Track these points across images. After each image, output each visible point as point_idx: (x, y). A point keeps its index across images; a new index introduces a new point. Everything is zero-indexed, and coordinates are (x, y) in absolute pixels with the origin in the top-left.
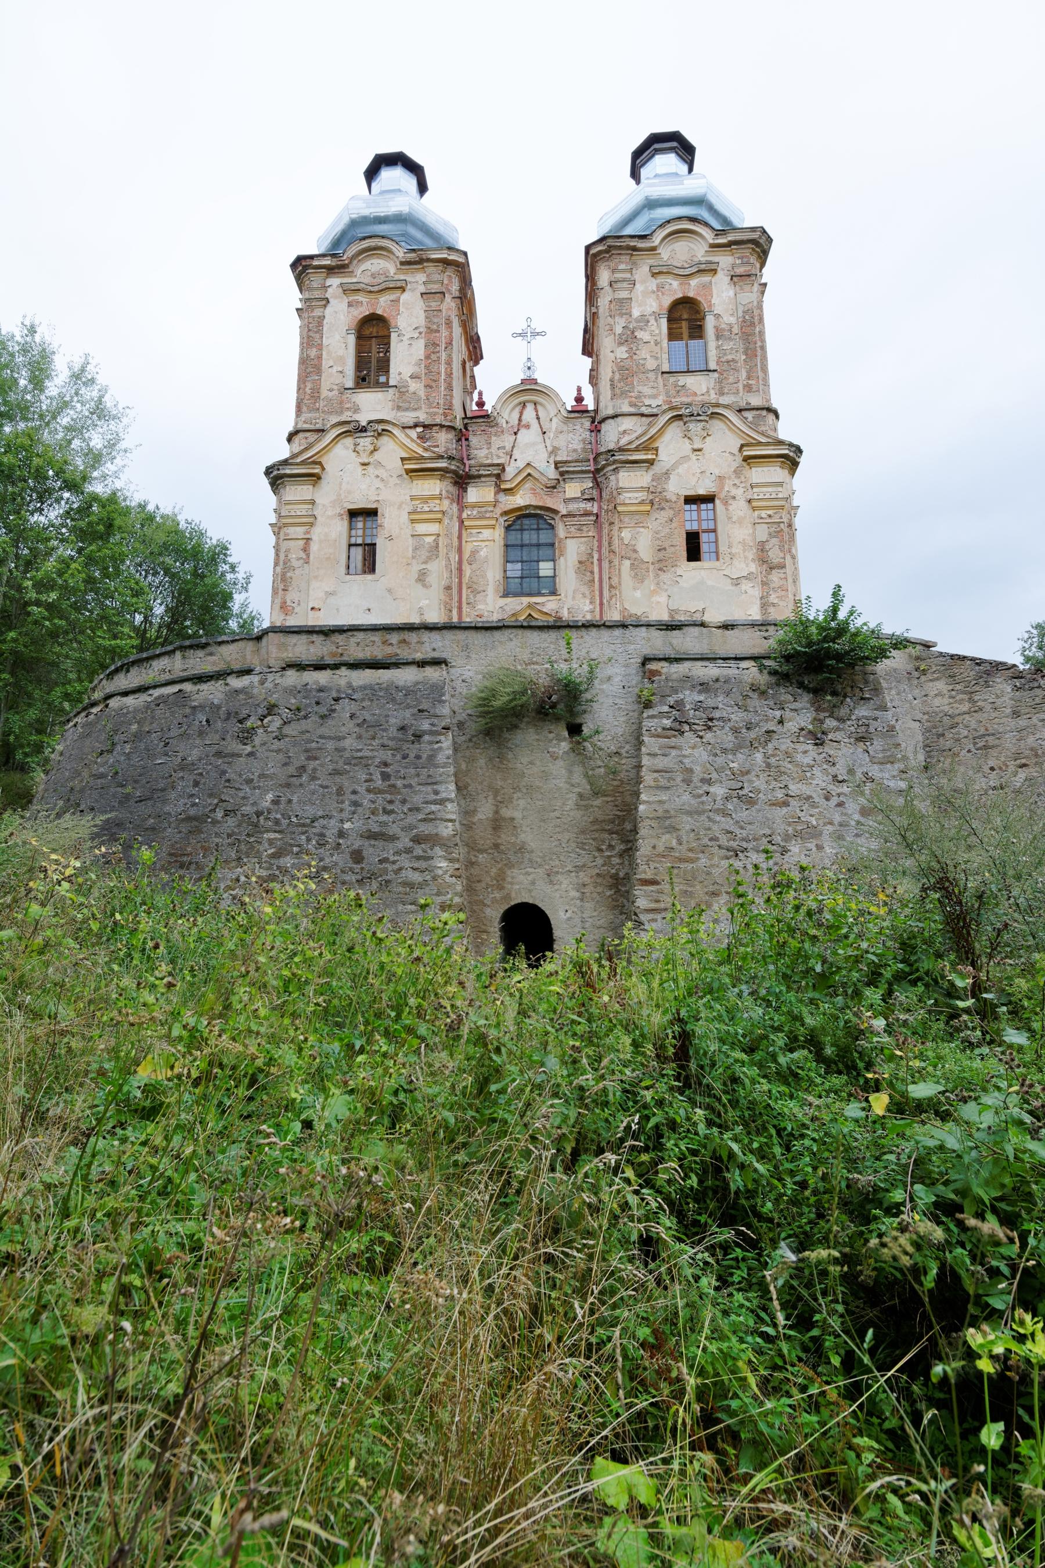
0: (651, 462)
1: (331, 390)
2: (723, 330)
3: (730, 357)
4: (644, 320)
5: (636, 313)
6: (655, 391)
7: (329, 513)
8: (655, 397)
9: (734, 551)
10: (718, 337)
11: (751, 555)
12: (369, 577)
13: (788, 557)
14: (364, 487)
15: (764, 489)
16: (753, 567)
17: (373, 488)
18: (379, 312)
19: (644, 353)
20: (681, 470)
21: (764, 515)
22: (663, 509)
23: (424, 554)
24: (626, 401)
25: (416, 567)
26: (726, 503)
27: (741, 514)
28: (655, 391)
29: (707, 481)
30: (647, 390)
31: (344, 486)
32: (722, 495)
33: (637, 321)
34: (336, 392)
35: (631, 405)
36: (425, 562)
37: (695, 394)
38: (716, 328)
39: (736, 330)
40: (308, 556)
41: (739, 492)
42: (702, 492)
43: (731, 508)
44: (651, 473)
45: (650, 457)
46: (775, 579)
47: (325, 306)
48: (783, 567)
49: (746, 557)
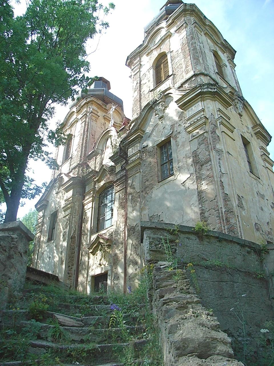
13: (213, 154)
26: (176, 138)
43: (178, 140)
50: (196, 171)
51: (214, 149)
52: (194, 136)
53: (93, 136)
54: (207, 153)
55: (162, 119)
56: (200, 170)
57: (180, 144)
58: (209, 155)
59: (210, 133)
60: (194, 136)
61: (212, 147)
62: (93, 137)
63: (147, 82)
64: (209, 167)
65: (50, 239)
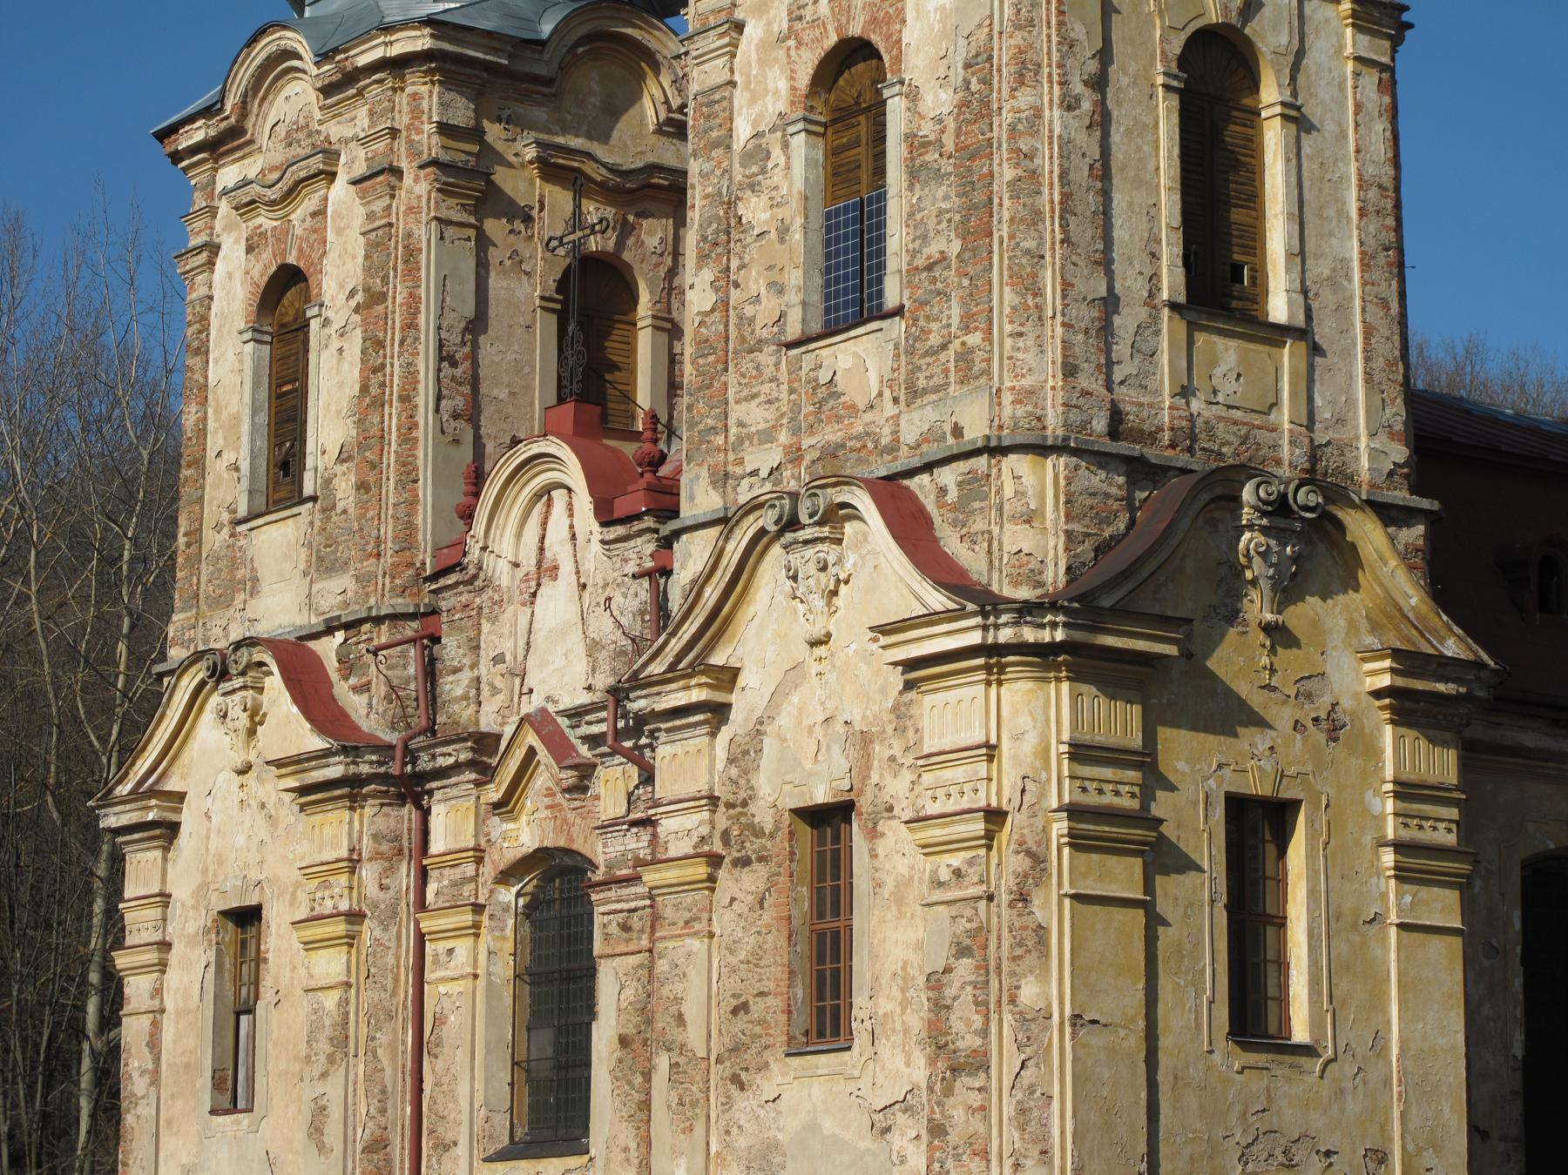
0: (718, 713)
1: (218, 527)
2: (925, 145)
3: (933, 249)
4: (757, 154)
5: (743, 130)
6: (770, 414)
7: (191, 928)
8: (767, 436)
9: (885, 1005)
10: (914, 174)
11: (916, 1021)
12: (244, 1119)
14: (241, 840)
15: (948, 774)
16: (919, 1072)
17: (256, 840)
18: (291, 259)
19: (754, 281)
20: (784, 720)
21: (945, 875)
22: (743, 862)
23: (324, 1047)
24: (704, 473)
25: (309, 1093)
26: (873, 834)
27: (901, 866)
28: (770, 414)
29: (836, 751)
30: (755, 415)
31: (212, 846)
32: (864, 804)
33: (749, 157)
34: (226, 531)
35: (722, 479)
36: (324, 1075)
37: (853, 409)
38: (910, 138)
39: (949, 144)
40: (157, 1060)
41: (897, 787)
42: (821, 795)
43: (882, 847)
44: (725, 733)
45: (696, 695)
46: (958, 1114)
47: (211, 264)
48: (979, 1063)
49: (906, 1031)
50: (931, 1089)
51: (1013, 1001)
52: (940, 884)
53: (454, 364)
54: (978, 1021)
55: (821, 651)
56: (948, 1092)
57: (890, 884)
58: (984, 1033)
59: (1005, 898)
60: (940, 884)
61: (1005, 989)
62: (458, 372)
63: (773, 235)
64: (976, 1099)
65: (223, 1080)
